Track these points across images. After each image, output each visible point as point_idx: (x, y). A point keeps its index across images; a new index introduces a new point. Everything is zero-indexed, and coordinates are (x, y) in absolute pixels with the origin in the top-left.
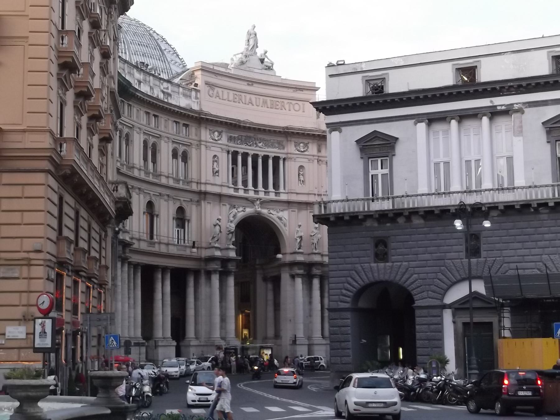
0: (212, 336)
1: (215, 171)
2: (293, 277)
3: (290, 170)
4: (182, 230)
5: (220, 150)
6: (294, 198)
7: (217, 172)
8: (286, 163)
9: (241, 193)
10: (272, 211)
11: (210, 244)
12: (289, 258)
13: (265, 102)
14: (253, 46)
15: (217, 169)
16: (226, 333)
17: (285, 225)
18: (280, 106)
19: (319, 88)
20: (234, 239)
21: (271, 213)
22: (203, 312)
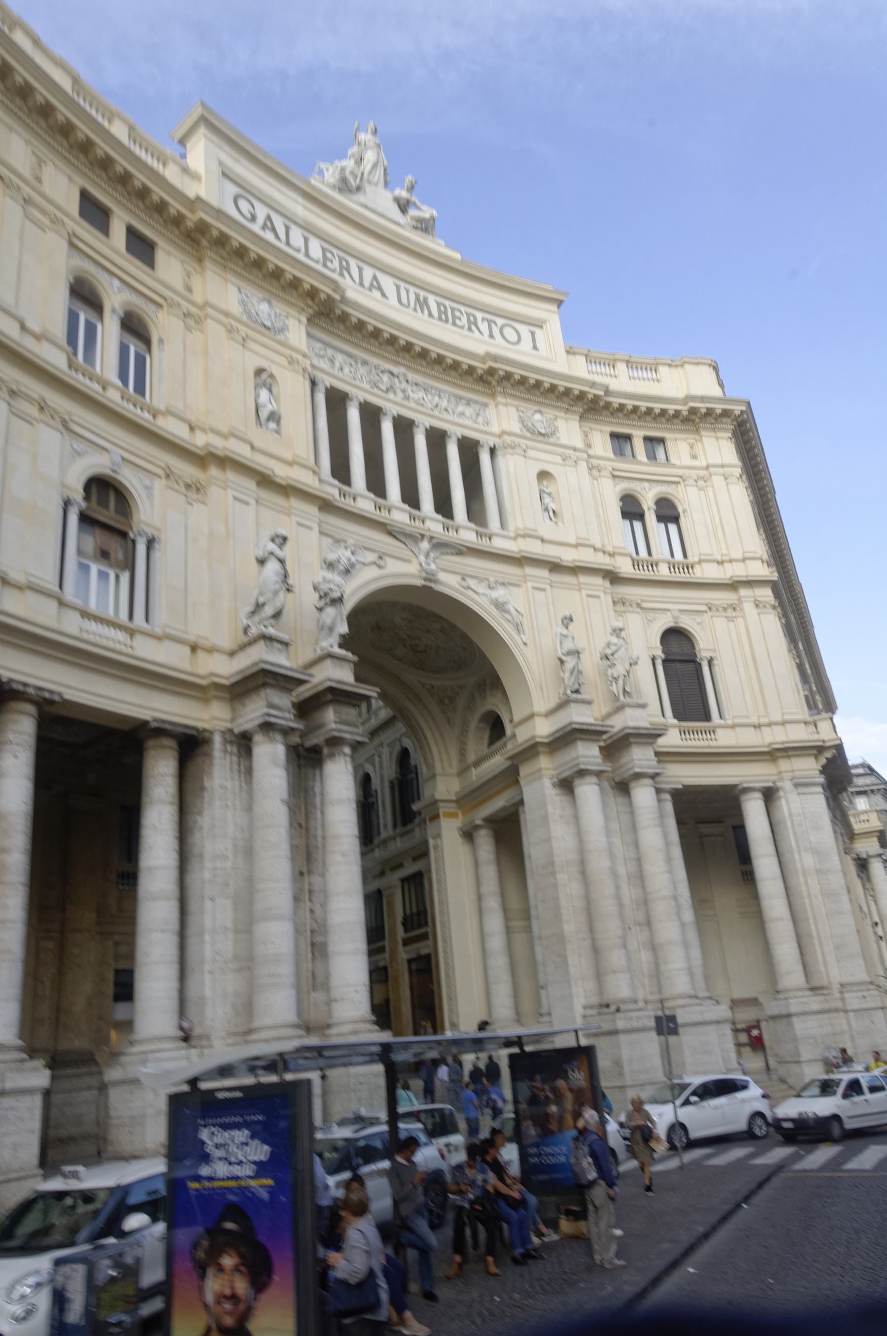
0: (256, 1024)
1: (264, 414)
2: (566, 785)
3: (511, 477)
4: (125, 577)
5: (284, 361)
6: (534, 548)
7: (274, 417)
8: (500, 460)
9: (366, 504)
10: (472, 583)
11: (246, 630)
12: (543, 729)
13: (422, 304)
14: (375, 165)
15: (270, 408)
16: (329, 1002)
17: (518, 628)
18: (464, 320)
19: (566, 294)
20: (343, 628)
21: (469, 588)
22: (215, 914)
